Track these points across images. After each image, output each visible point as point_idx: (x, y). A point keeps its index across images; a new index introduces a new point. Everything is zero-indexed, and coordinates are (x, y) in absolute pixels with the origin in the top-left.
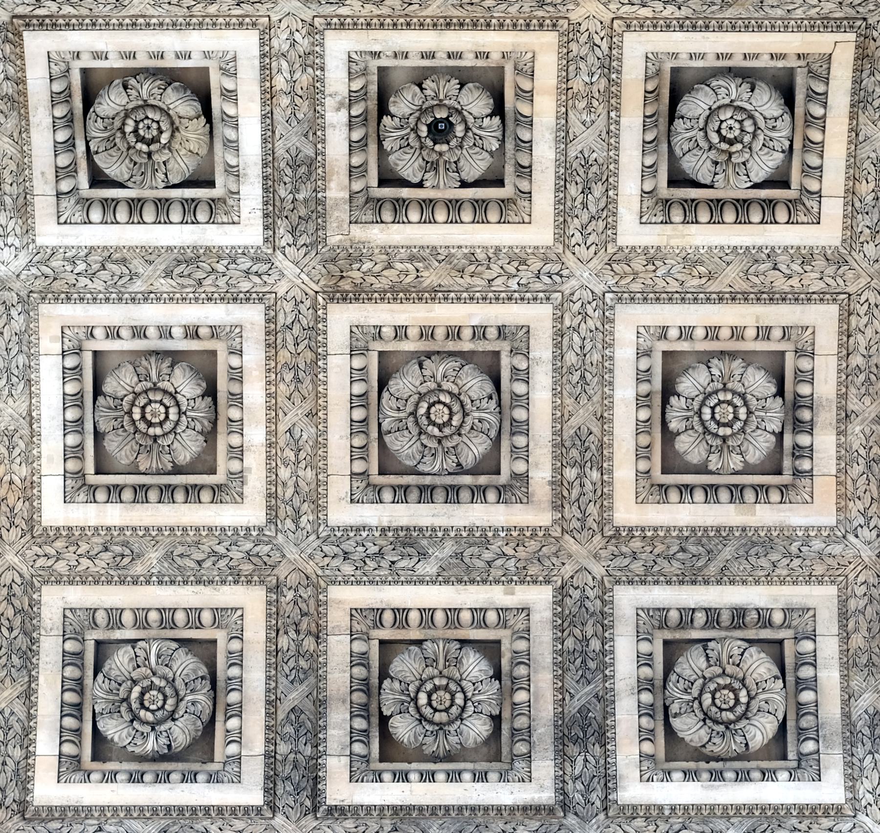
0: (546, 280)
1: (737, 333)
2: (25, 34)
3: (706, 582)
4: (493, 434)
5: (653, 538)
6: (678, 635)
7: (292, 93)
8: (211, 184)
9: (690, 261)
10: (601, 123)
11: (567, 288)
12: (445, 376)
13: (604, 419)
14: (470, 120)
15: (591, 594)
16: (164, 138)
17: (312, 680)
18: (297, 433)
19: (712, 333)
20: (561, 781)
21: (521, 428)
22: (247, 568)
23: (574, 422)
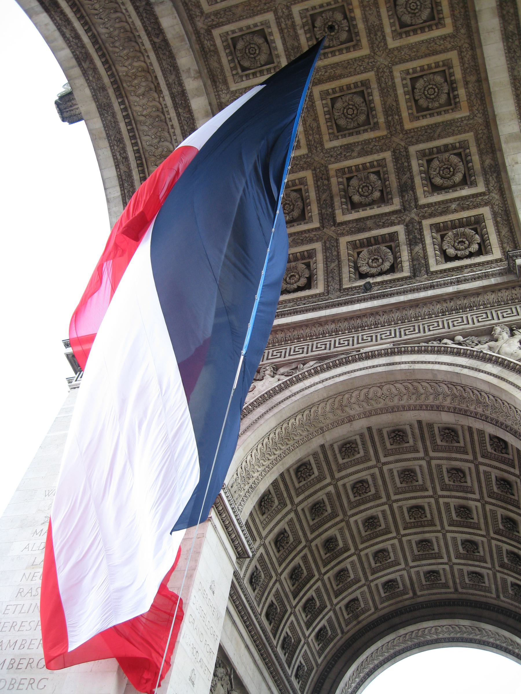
0: (370, 64)
2: (212, 31)
3: (435, 140)
4: (366, 113)
5: (417, 131)
6: (430, 157)
7: (287, 28)
8: (273, 63)
9: (410, 47)
10: (375, 13)
12: (349, 100)
13: (397, 101)
15: (402, 150)
16: (257, 52)
17: (328, 192)
18: (311, 125)
19: (422, 68)
21: (373, 109)
22: (305, 166)
23: (388, 103)
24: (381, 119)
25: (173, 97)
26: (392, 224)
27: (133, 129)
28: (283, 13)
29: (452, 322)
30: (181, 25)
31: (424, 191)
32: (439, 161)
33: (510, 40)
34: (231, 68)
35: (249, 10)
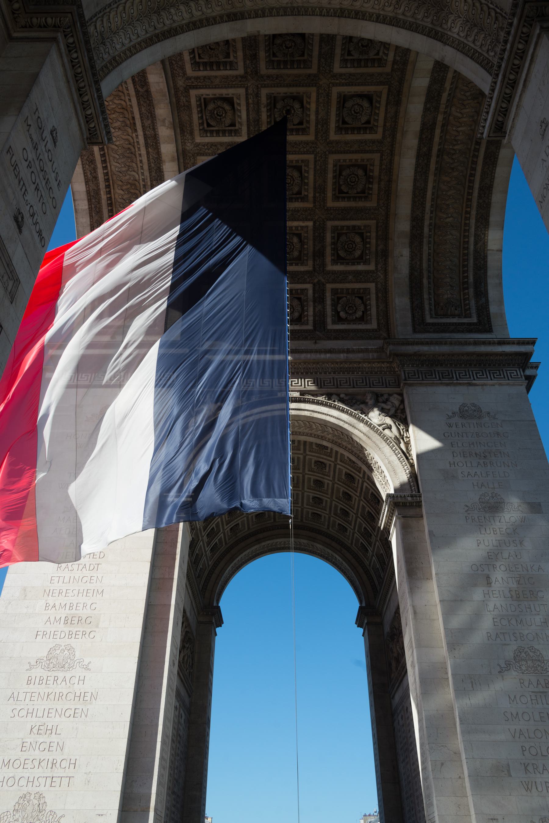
1: (356, 160)
2: (190, 90)
3: (347, 220)
8: (235, 126)
11: (317, 150)
14: (295, 109)
19: (351, 160)
20: (314, 265)
21: (307, 184)
24: (311, 195)
25: (146, 137)
26: (304, 282)
27: (104, 153)
28: (254, 91)
29: (340, 381)
30: (165, 84)
31: (332, 259)
32: (347, 237)
33: (422, 158)
34: (199, 123)
35: (226, 82)
